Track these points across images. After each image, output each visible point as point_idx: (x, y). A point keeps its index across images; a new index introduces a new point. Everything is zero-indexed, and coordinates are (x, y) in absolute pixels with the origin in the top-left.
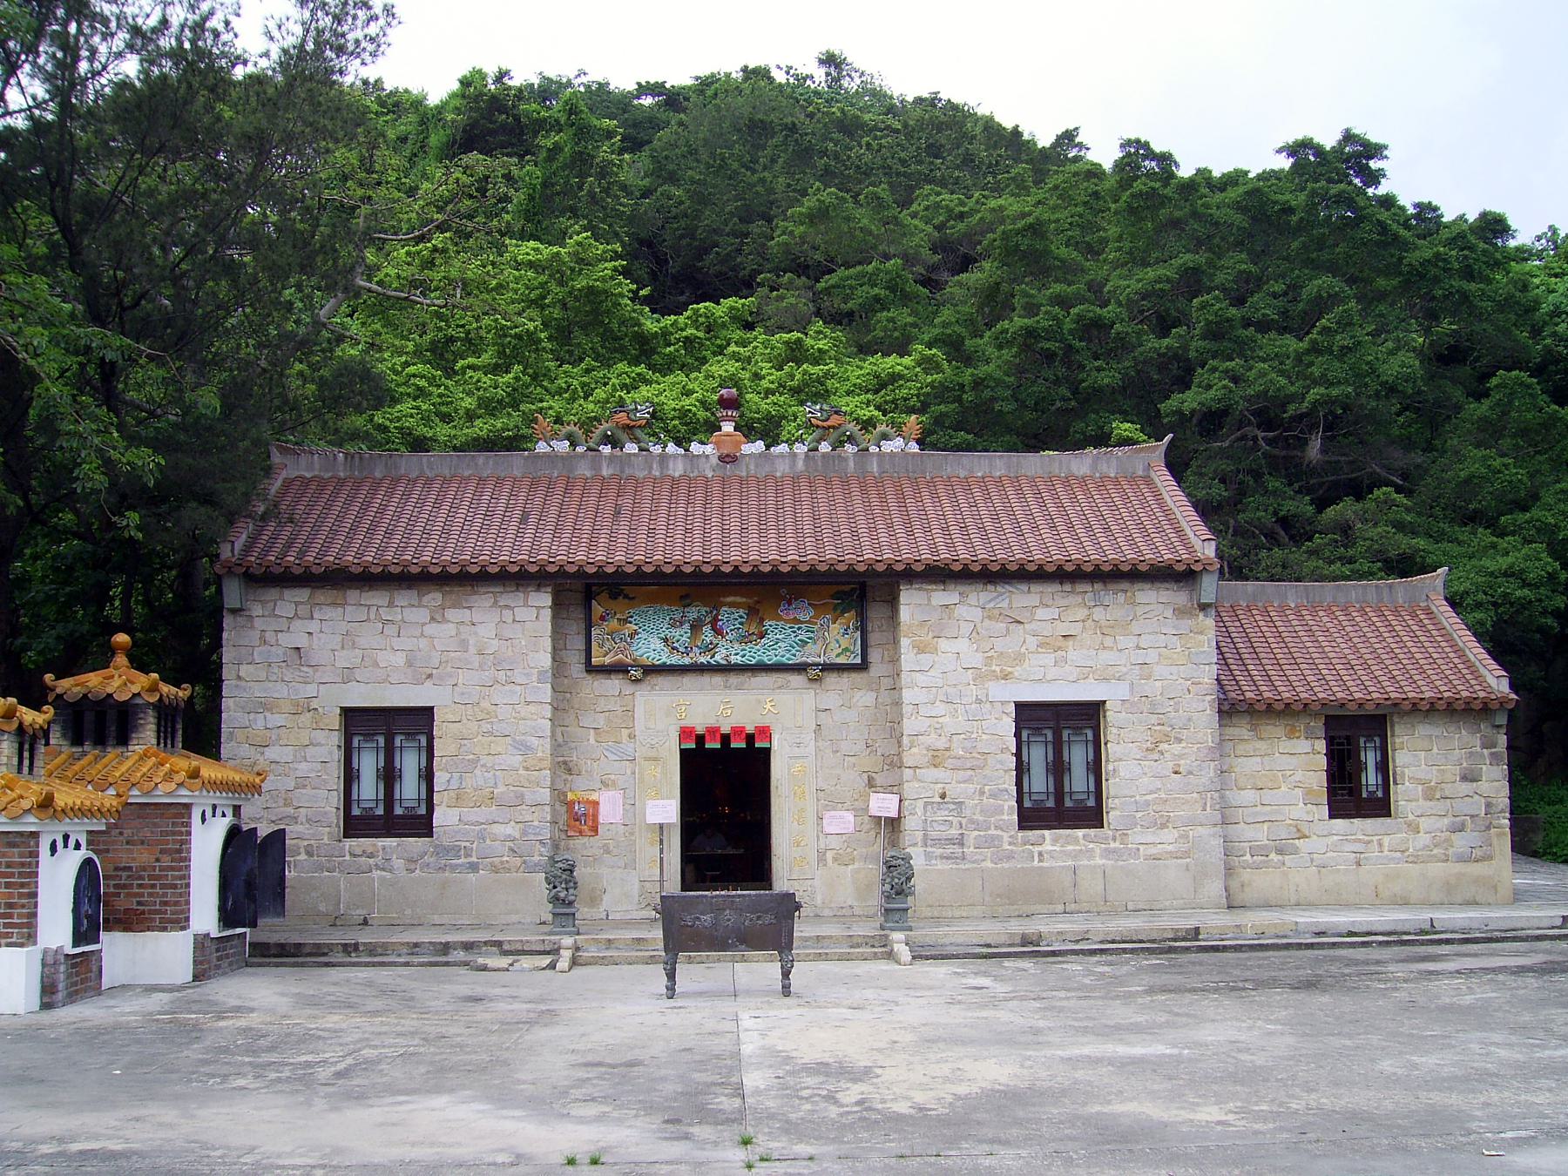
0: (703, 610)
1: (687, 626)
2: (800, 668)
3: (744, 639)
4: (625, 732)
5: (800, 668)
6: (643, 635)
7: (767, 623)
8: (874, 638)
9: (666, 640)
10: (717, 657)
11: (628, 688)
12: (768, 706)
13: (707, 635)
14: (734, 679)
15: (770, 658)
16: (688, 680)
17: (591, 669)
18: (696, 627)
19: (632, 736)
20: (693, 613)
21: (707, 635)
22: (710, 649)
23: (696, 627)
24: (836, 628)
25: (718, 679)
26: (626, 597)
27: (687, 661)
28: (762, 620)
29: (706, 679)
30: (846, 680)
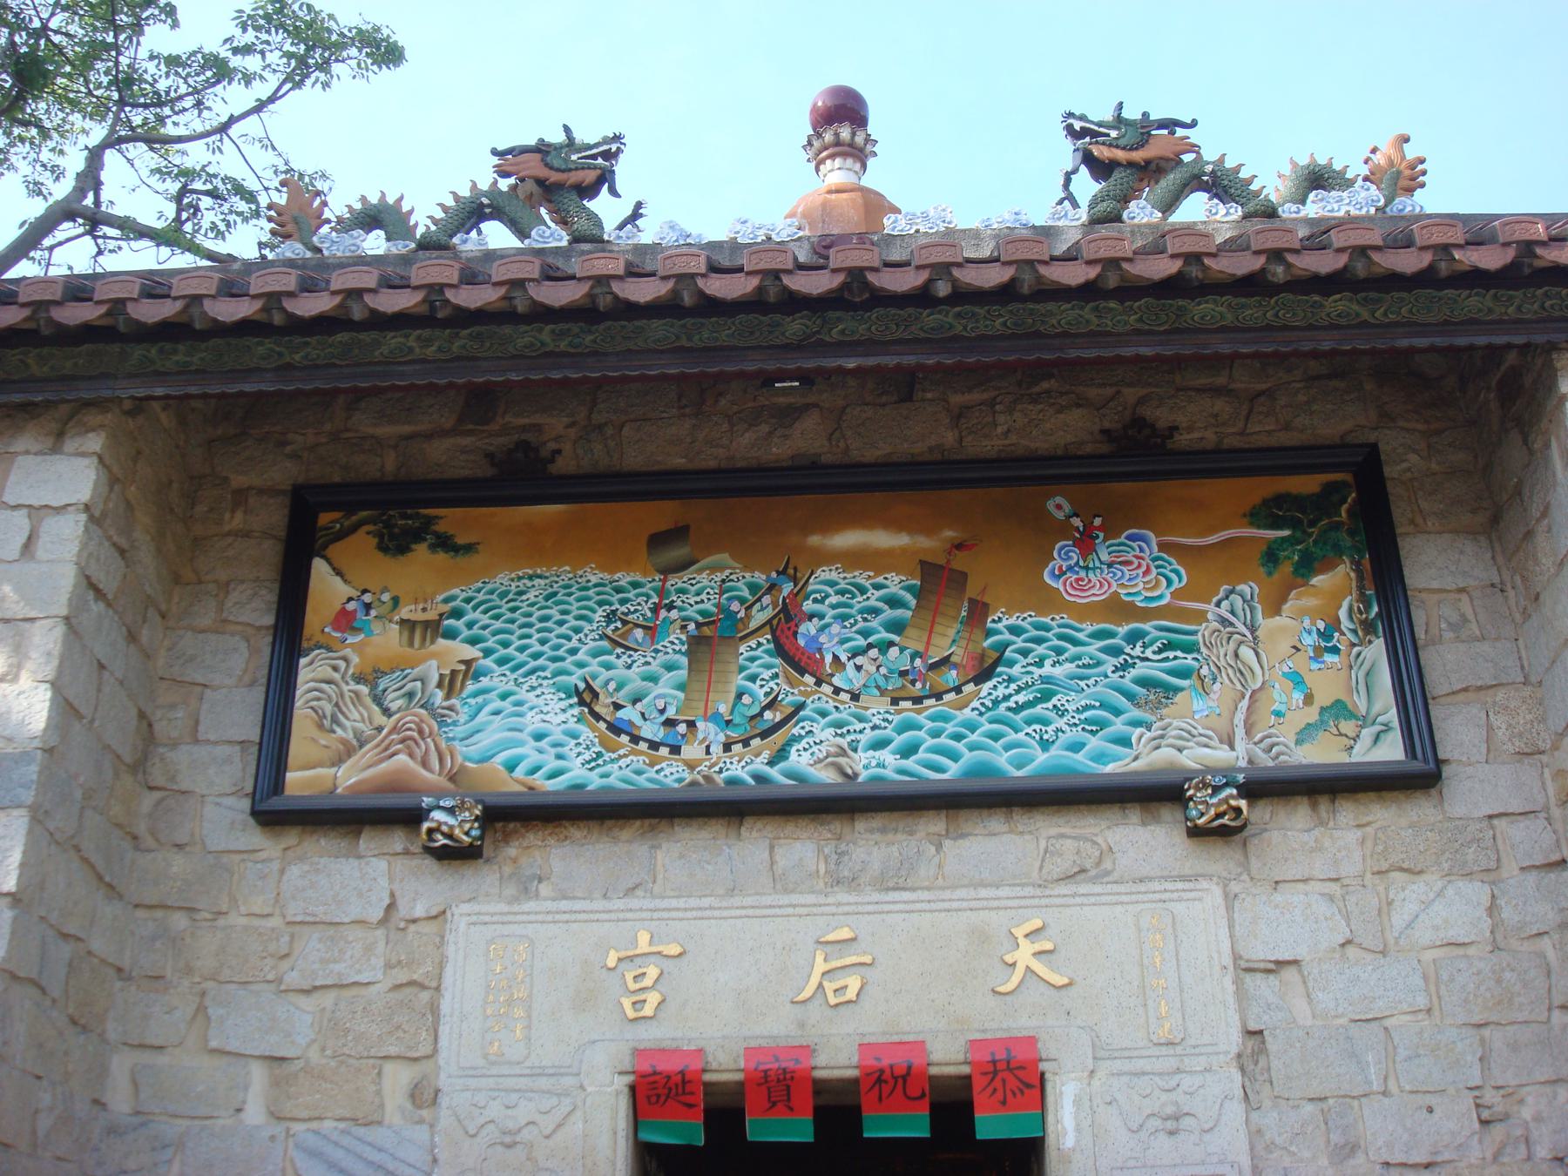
0: (743, 581)
1: (674, 642)
2: (1156, 795)
3: (910, 690)
4: (398, 1079)
5: (1156, 795)
6: (498, 679)
7: (1002, 621)
8: (1445, 664)
9: (586, 697)
10: (799, 759)
11: (425, 888)
12: (1024, 954)
13: (755, 671)
14: (872, 846)
15: (1023, 758)
16: (682, 853)
17: (278, 814)
18: (709, 643)
19: (424, 1097)
20: (700, 591)
21: (755, 671)
22: (771, 727)
23: (709, 643)
24: (1289, 629)
25: (801, 848)
26: (444, 543)
27: (670, 776)
28: (978, 612)
29: (752, 847)
30: (1344, 837)
